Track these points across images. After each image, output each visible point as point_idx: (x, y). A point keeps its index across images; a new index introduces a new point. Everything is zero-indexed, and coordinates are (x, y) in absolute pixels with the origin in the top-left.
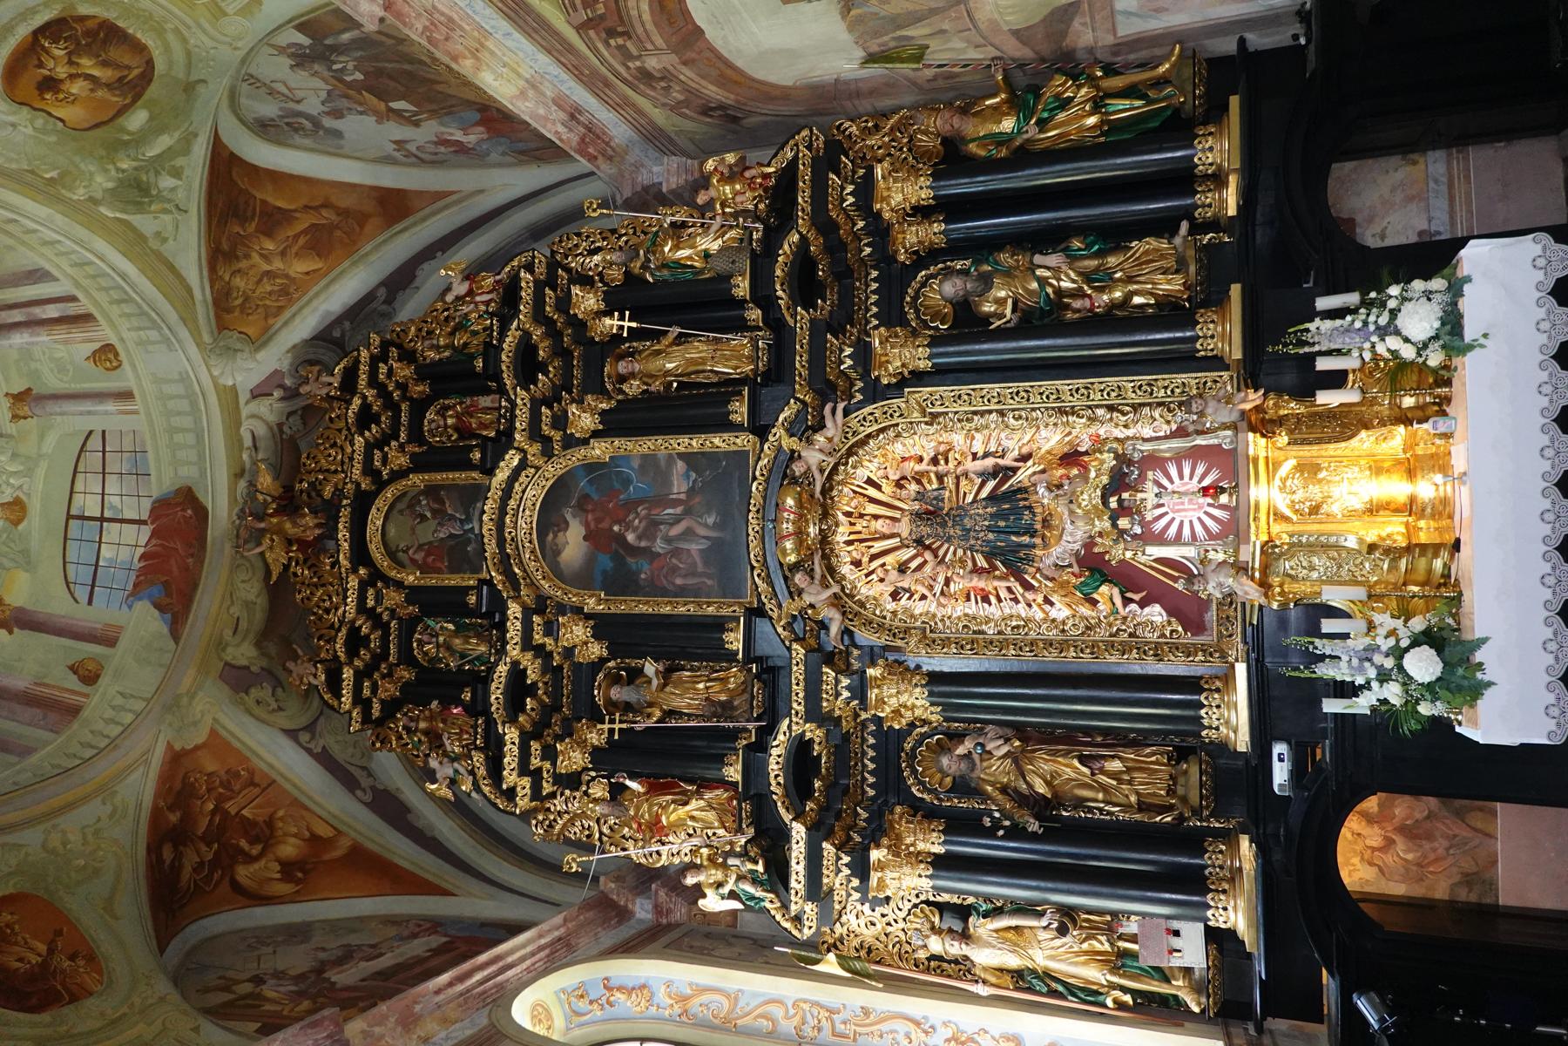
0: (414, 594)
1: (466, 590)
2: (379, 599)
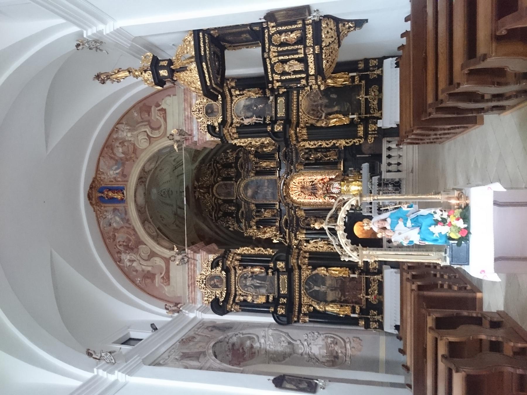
0: (223, 200)
1: (233, 200)
2: (217, 201)
